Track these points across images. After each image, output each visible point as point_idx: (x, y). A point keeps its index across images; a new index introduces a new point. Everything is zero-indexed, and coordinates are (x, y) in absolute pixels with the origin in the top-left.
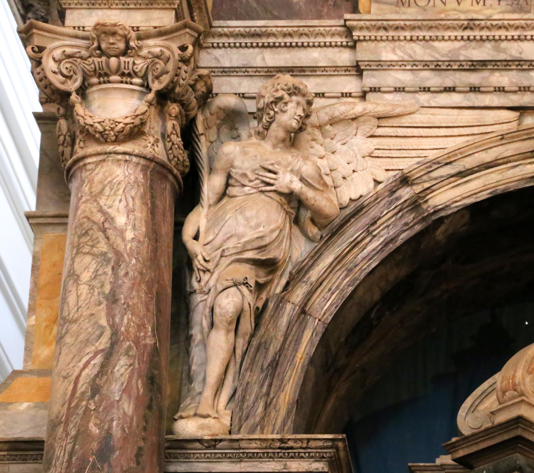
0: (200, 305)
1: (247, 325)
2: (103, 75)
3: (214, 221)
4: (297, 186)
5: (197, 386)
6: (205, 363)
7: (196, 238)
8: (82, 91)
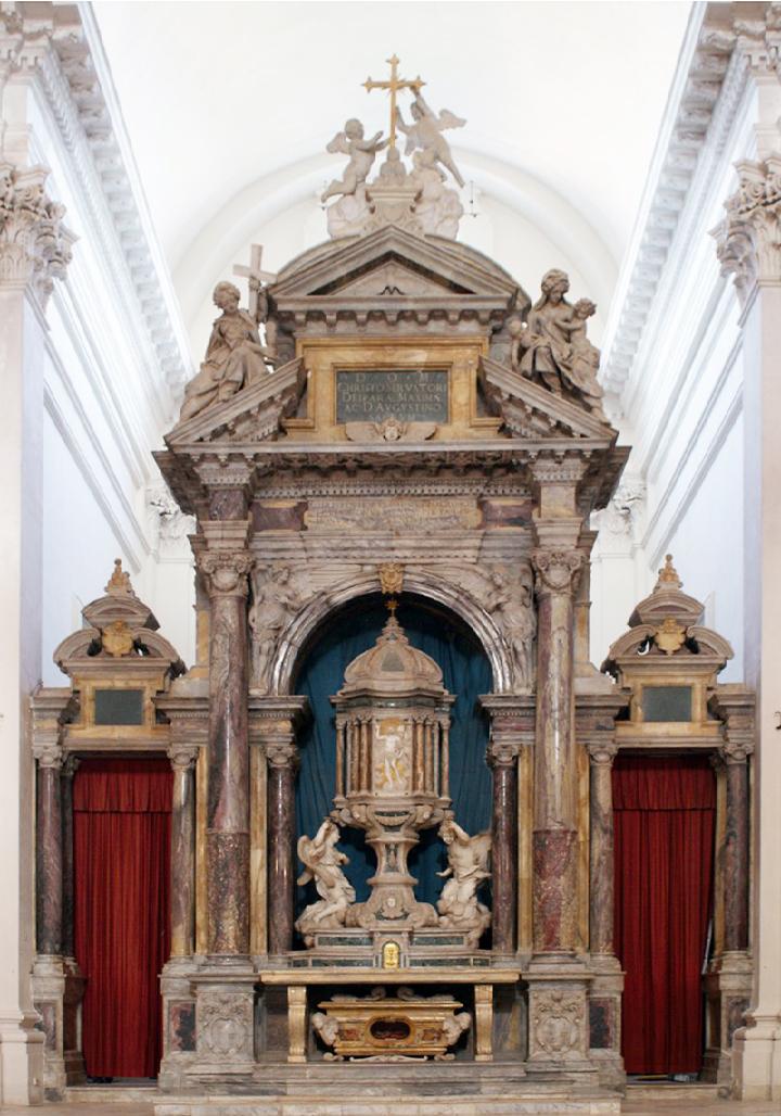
0: (256, 644)
1: (272, 652)
2: (222, 567)
3: (260, 614)
4: (287, 601)
5: (256, 673)
6: (258, 666)
7: (253, 621)
8: (214, 572)
